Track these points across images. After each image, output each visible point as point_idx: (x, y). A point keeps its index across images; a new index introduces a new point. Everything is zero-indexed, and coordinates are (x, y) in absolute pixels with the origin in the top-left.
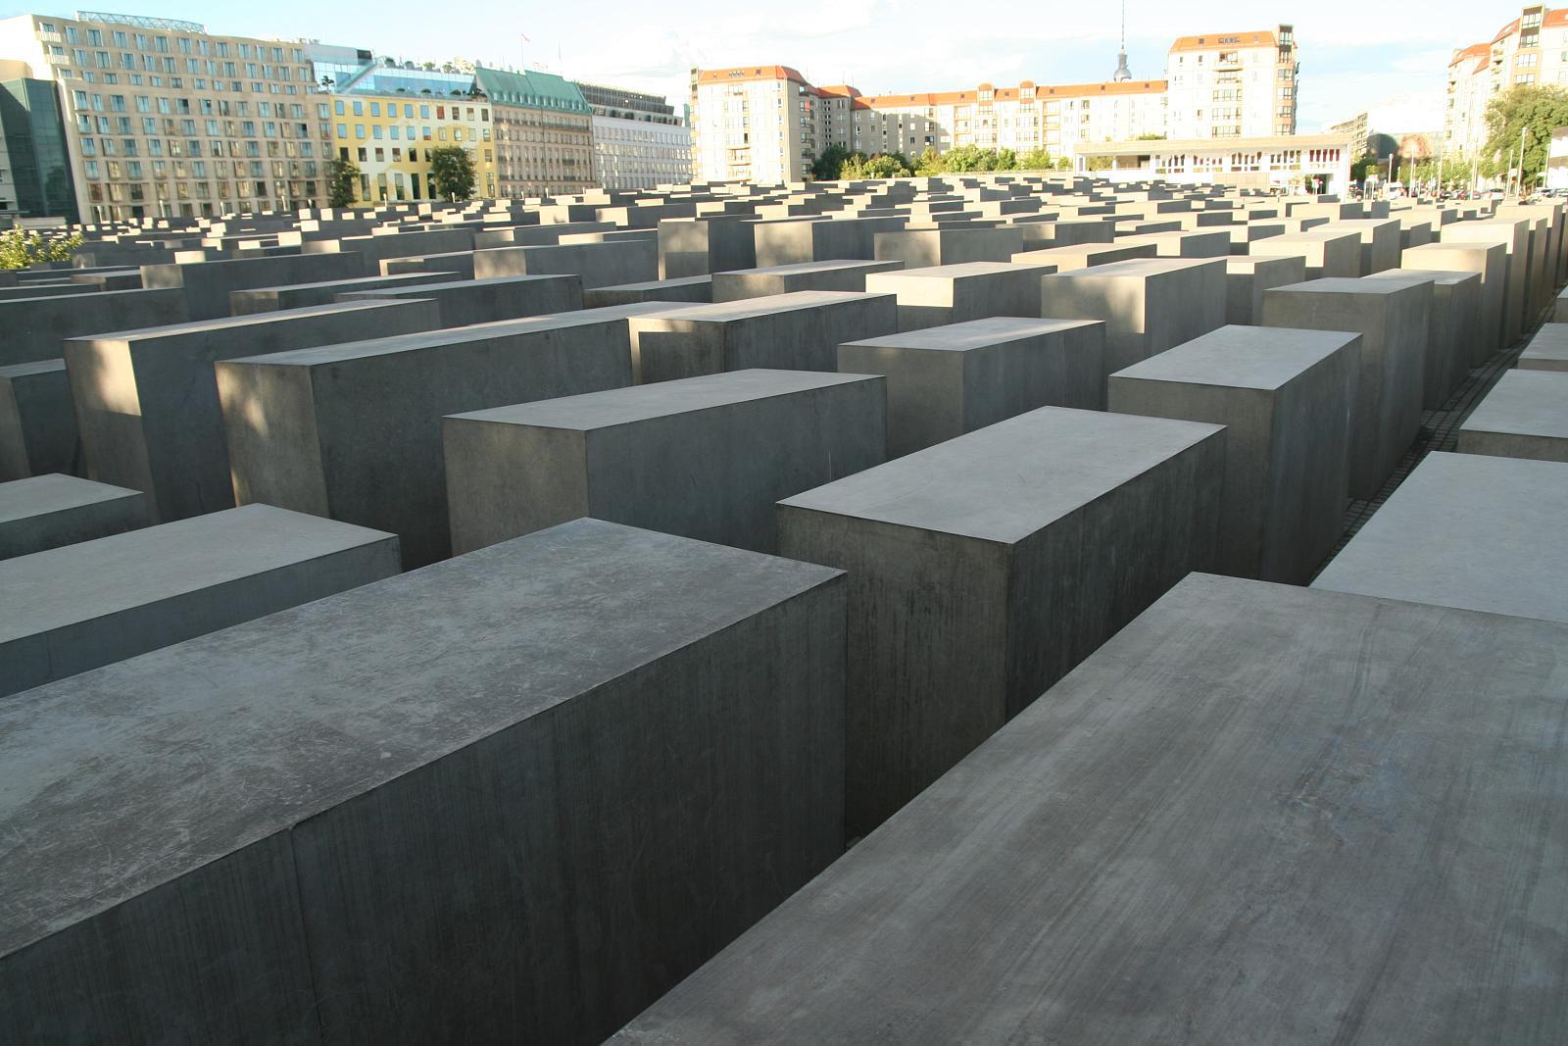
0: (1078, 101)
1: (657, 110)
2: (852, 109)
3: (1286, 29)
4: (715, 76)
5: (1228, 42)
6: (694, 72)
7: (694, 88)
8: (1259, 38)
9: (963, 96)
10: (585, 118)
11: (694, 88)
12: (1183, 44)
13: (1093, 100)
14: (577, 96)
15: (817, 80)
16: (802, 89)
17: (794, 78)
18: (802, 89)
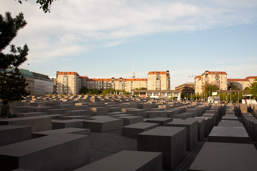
0: (130, 82)
1: (46, 78)
2: (87, 81)
3: (168, 71)
4: (62, 73)
5: (158, 73)
6: (57, 72)
7: (57, 75)
8: (163, 73)
9: (109, 80)
10: (33, 79)
11: (57, 75)
12: (150, 73)
13: (133, 82)
14: (32, 75)
15: (81, 75)
16: (78, 77)
17: (76, 74)
18: (78, 77)
